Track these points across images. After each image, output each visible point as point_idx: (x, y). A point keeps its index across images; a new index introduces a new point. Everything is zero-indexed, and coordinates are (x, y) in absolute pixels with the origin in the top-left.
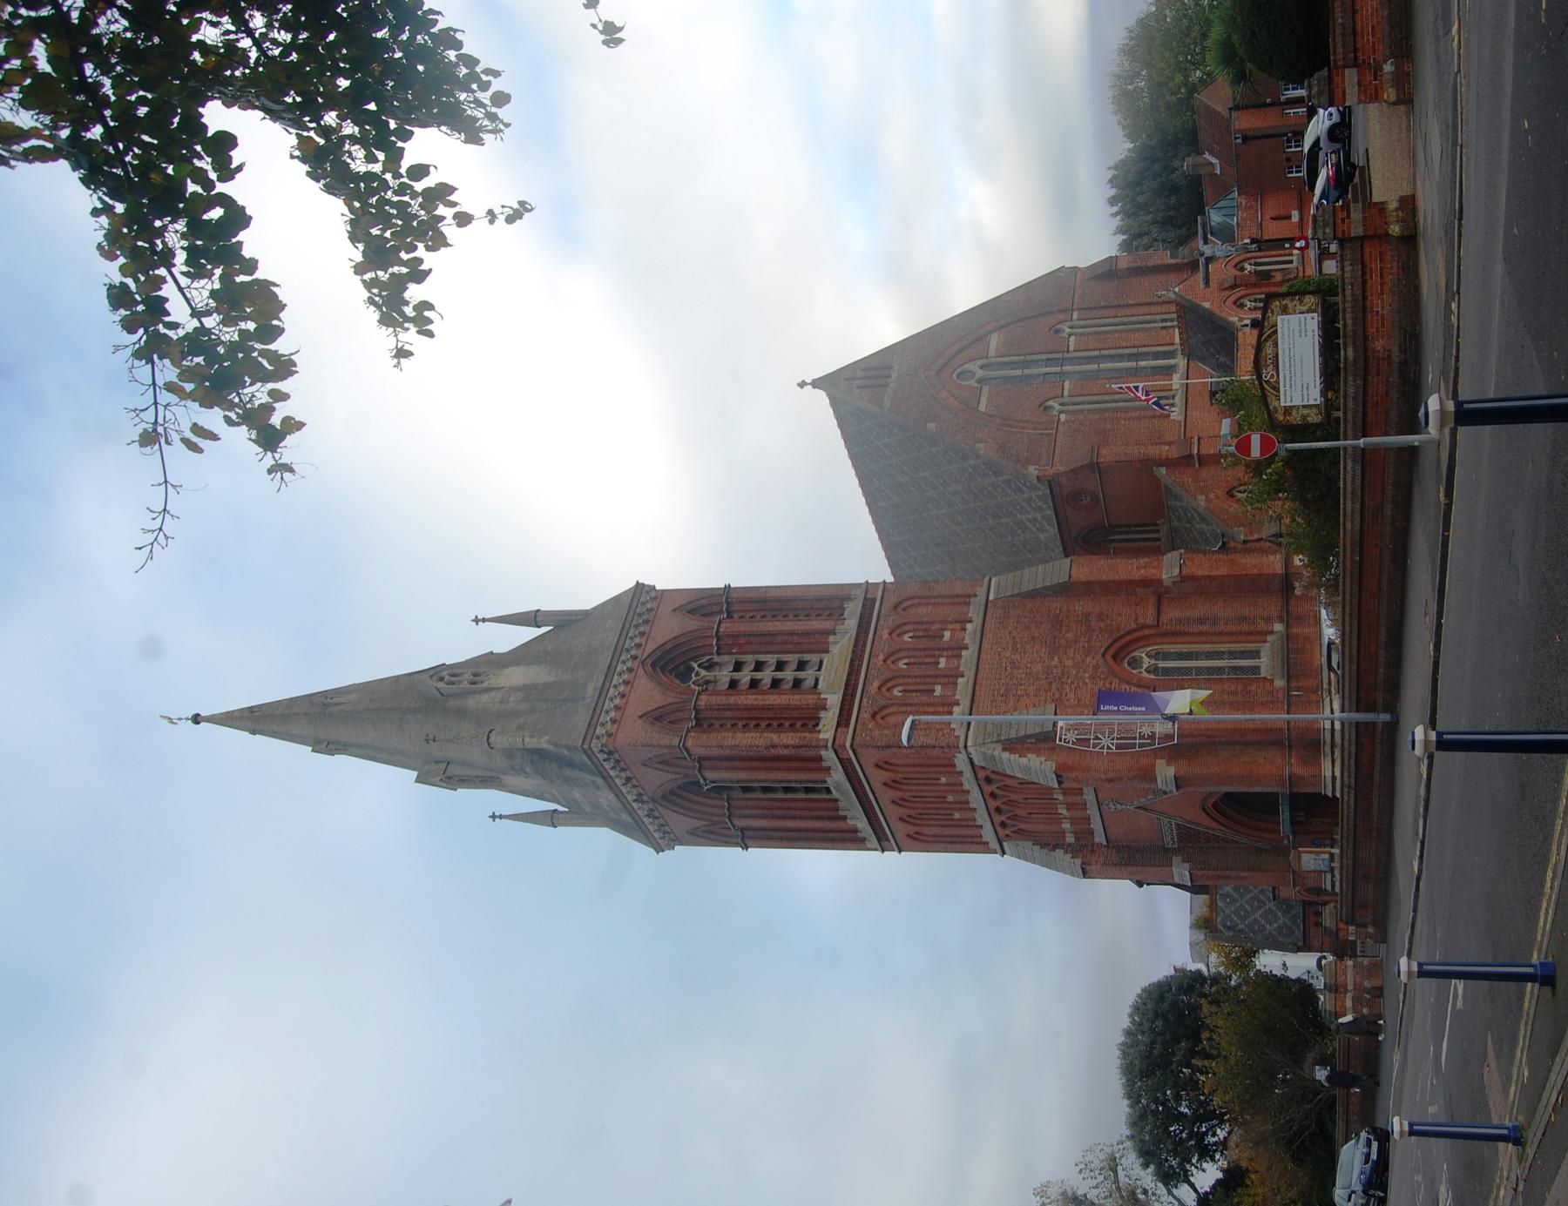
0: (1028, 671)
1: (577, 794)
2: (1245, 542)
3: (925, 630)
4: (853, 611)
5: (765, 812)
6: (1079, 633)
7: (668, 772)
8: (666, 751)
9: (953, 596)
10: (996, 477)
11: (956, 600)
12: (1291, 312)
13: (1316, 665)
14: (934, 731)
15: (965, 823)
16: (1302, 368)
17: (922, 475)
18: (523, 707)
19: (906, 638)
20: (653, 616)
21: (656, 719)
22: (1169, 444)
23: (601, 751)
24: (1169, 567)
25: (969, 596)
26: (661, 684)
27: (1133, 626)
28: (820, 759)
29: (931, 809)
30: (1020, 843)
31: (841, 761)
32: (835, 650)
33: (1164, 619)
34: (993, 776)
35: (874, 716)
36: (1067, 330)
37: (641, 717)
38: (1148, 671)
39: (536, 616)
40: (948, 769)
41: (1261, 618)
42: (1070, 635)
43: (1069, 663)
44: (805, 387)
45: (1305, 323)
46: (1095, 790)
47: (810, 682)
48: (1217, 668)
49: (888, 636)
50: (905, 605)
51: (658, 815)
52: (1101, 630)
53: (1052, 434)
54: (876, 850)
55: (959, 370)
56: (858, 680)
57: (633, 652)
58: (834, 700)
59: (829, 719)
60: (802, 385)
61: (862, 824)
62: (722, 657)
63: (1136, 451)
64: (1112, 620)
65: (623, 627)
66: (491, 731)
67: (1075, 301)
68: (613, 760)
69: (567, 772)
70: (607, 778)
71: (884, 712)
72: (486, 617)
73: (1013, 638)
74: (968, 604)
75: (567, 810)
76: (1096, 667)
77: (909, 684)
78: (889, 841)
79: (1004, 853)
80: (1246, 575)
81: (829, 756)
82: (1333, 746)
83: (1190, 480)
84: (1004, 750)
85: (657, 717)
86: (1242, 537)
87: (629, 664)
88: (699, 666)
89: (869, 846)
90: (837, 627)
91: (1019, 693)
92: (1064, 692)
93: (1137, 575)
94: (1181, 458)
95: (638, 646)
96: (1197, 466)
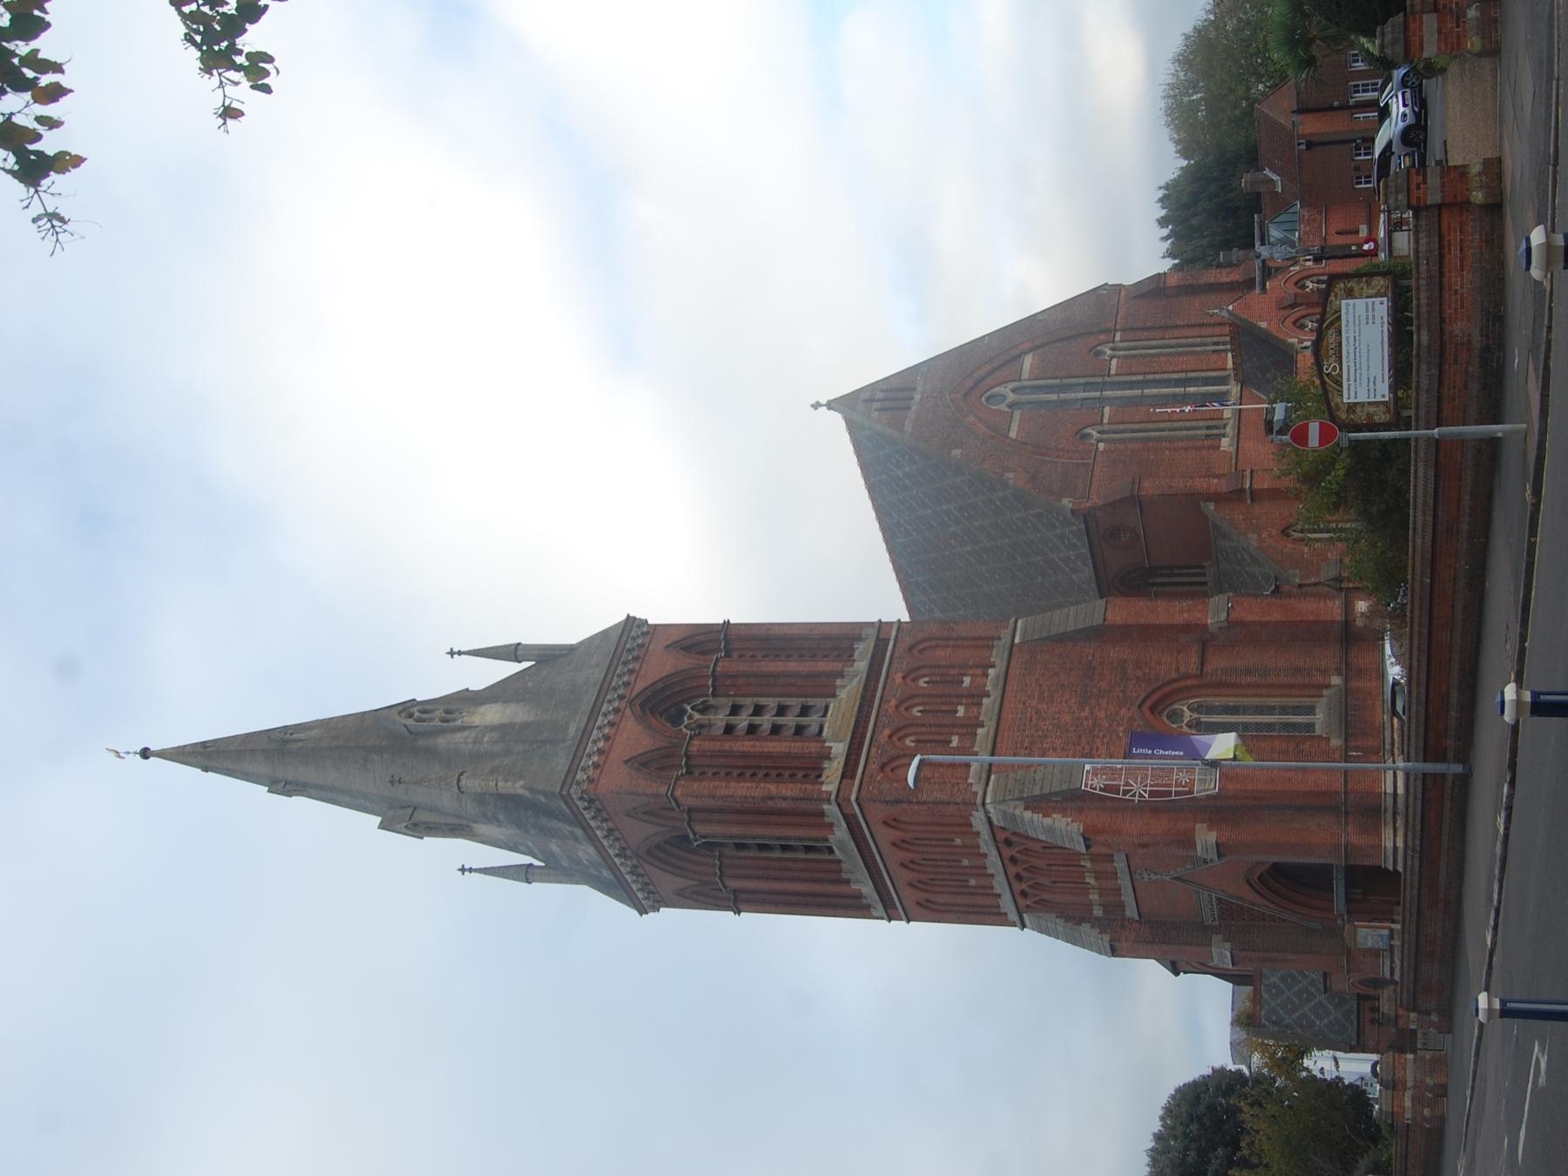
0: (1055, 722)
1: (554, 847)
2: (1300, 586)
3: (943, 675)
4: (864, 651)
5: (761, 872)
6: (1113, 682)
7: (653, 824)
8: (652, 800)
9: (975, 639)
10: (1026, 510)
11: (978, 643)
12: (1357, 296)
13: (1377, 724)
15: (982, 891)
16: (1368, 360)
17: (945, 507)
18: (497, 748)
19: (921, 683)
20: (643, 652)
21: (644, 764)
22: (1219, 476)
23: (581, 798)
24: (1215, 612)
25: (993, 639)
26: (649, 727)
27: (1174, 675)
28: (822, 814)
29: (943, 873)
30: (1041, 914)
31: (845, 816)
32: (843, 694)
33: (1208, 668)
34: (1014, 839)
35: (882, 768)
36: (1109, 352)
37: (626, 762)
38: (1189, 725)
39: (516, 650)
40: (964, 829)
41: (1318, 670)
42: (1103, 684)
43: (1101, 714)
44: (819, 408)
45: (1373, 309)
46: (1127, 855)
47: (814, 729)
48: (1266, 724)
49: (901, 680)
50: (921, 647)
51: (642, 872)
53: (1088, 464)
54: (882, 919)
55: (989, 393)
56: (867, 727)
57: (621, 691)
58: (839, 749)
59: (834, 769)
60: (816, 406)
61: (867, 889)
62: (716, 699)
63: (1181, 485)
64: (1150, 669)
65: (610, 664)
66: (462, 774)
67: (1119, 320)
68: (594, 809)
69: (544, 821)
70: (586, 829)
71: (895, 764)
72: (462, 650)
73: (1040, 686)
74: (991, 648)
75: (543, 864)
76: (1132, 719)
77: (922, 733)
78: (897, 909)
79: (1023, 926)
80: (1301, 621)
81: (831, 809)
82: (1395, 814)
83: (1241, 517)
84: (1027, 808)
85: (643, 763)
86: (1298, 580)
87: (616, 704)
88: (692, 708)
89: (874, 914)
90: (846, 669)
91: (1045, 745)
92: (1095, 747)
93: (1179, 619)
94: (1231, 492)
95: (626, 684)
96: (1249, 502)
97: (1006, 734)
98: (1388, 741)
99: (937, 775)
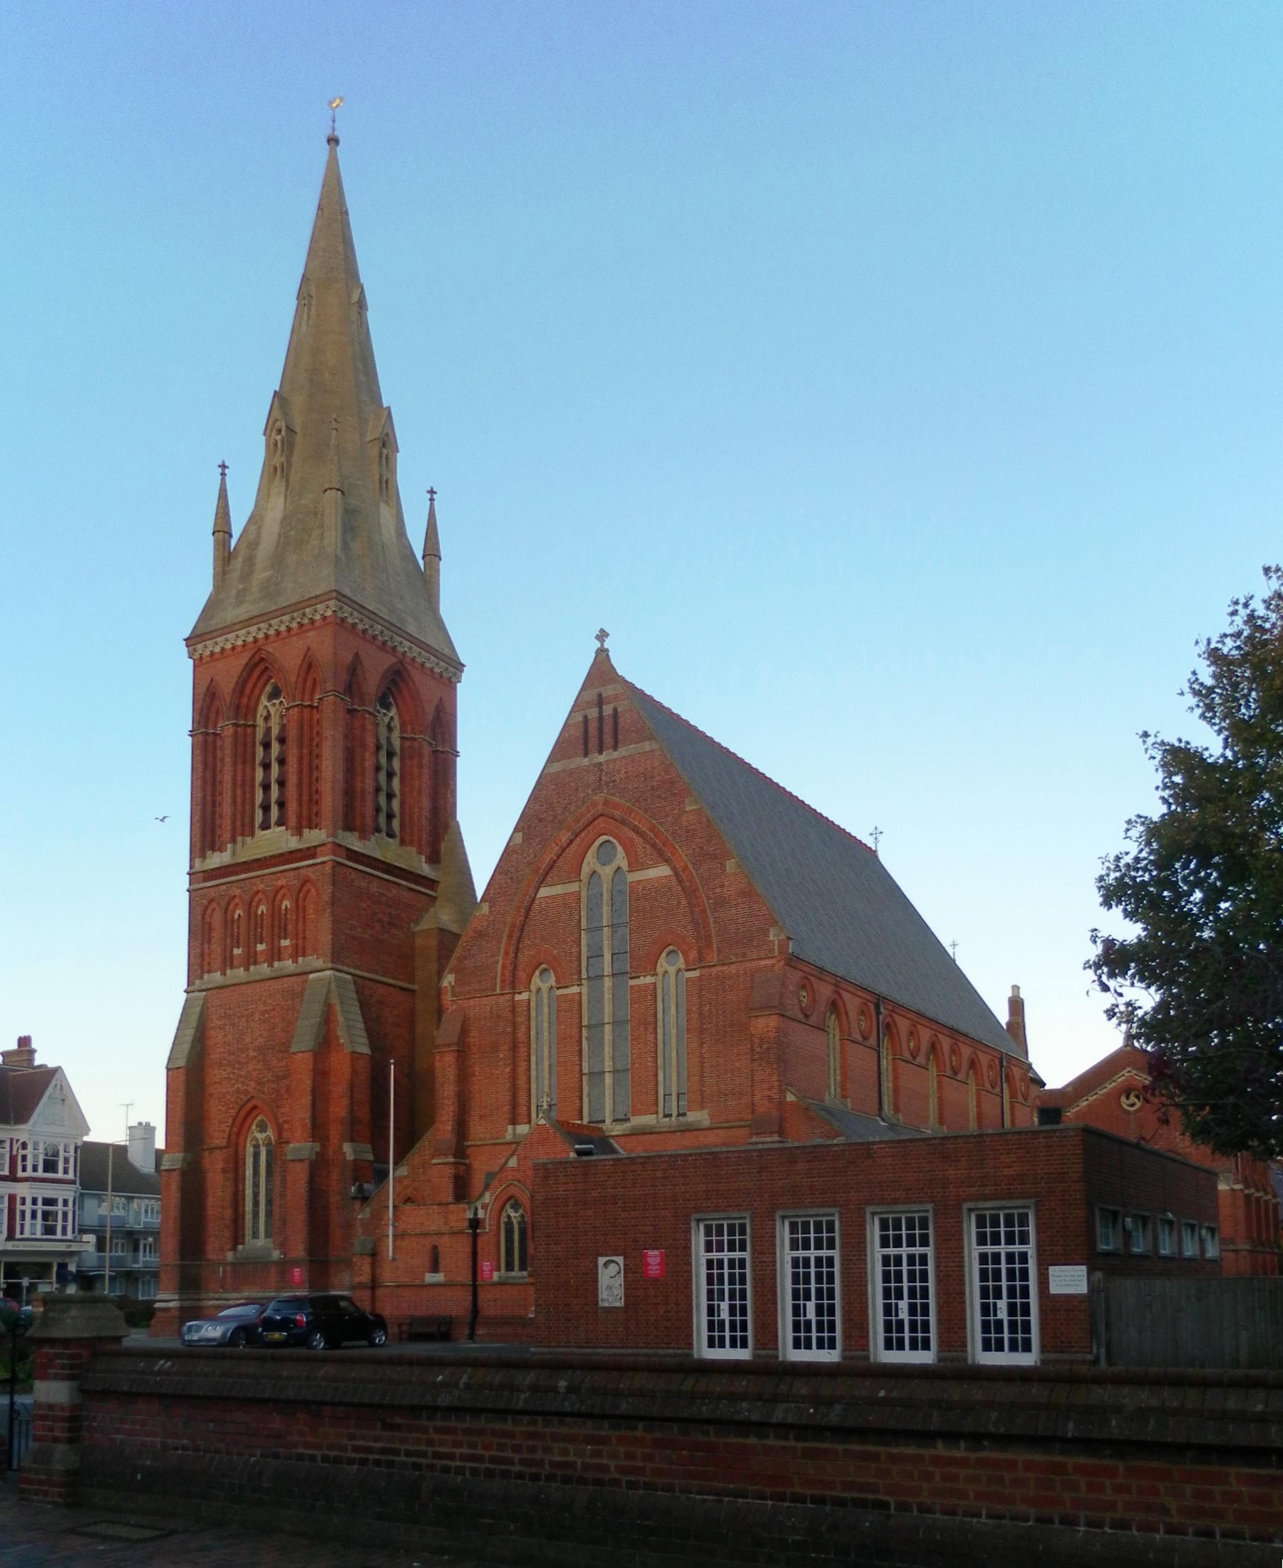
6: (276, 1070)
42: (274, 1062)
55: (614, 841)
67: (719, 968)
73: (274, 1009)
98: (227, 1296)
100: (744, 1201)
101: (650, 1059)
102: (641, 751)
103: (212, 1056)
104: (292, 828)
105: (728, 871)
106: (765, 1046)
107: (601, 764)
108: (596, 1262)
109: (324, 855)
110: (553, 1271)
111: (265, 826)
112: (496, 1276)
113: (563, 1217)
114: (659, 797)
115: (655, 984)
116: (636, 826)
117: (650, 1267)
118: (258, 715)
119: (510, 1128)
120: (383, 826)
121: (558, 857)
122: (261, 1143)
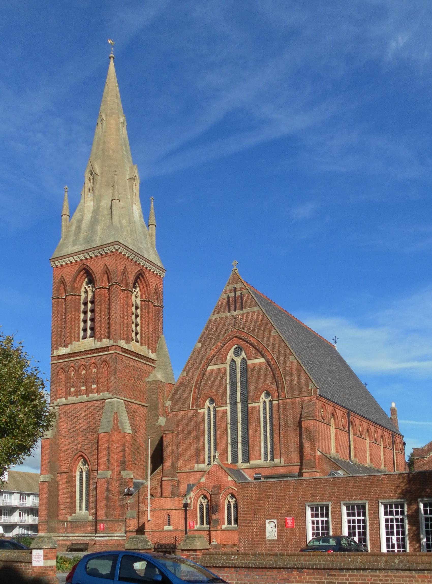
14: (55, 393)
42: (90, 437)
43: (79, 438)
49: (92, 363)
50: (107, 365)
52: (91, 449)
67: (288, 400)
73: (90, 414)
76: (77, 449)
91: (68, 422)
97: (72, 407)
99: (62, 387)
100: (327, 498)
101: (258, 437)
102: (252, 311)
103: (61, 434)
104: (98, 339)
105: (291, 360)
106: (309, 432)
107: (235, 316)
108: (265, 522)
109: (113, 350)
110: (246, 525)
111: (84, 338)
112: (196, 527)
113: (250, 504)
114: (260, 329)
115: (259, 406)
116: (251, 341)
117: (288, 524)
118: (82, 291)
119: (196, 465)
120: (134, 338)
121: (217, 353)
122: (83, 470)
